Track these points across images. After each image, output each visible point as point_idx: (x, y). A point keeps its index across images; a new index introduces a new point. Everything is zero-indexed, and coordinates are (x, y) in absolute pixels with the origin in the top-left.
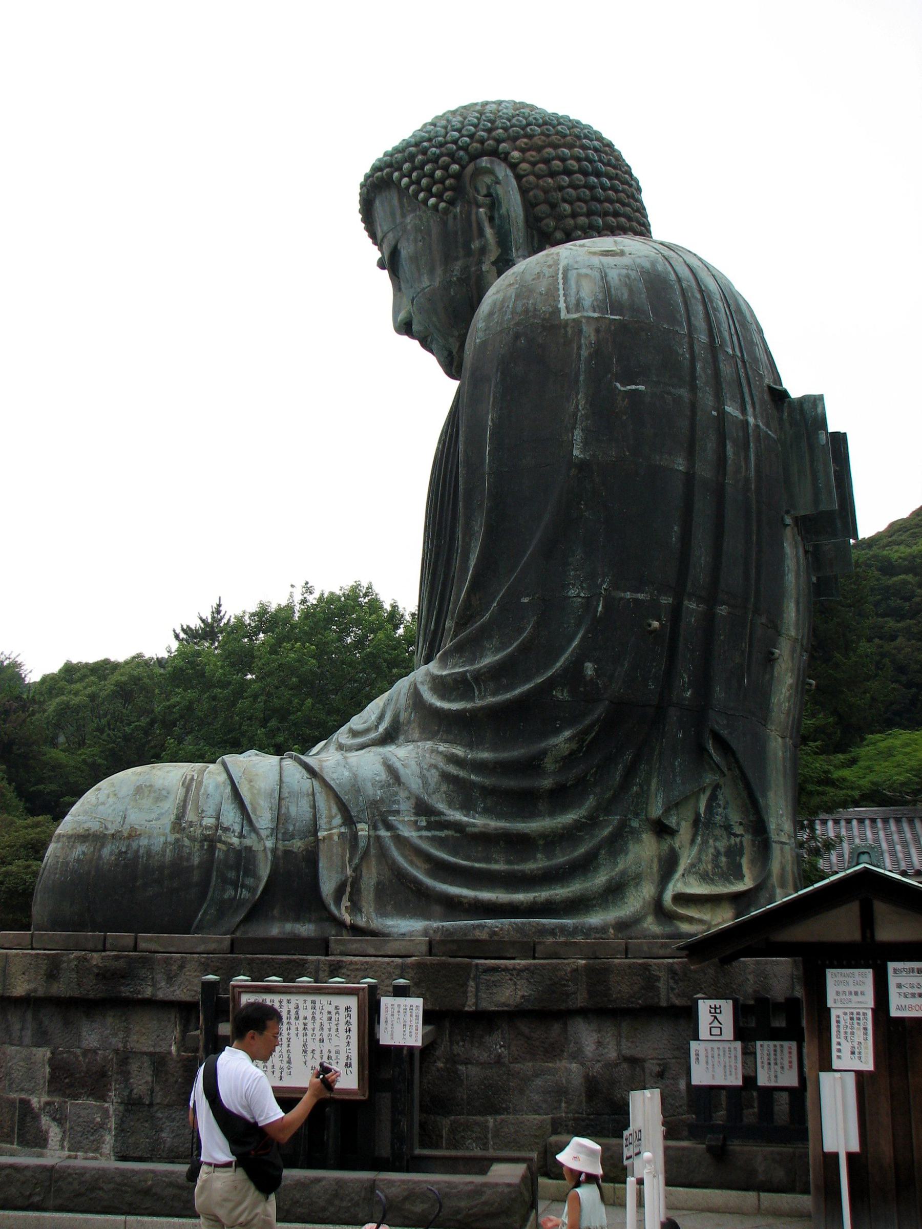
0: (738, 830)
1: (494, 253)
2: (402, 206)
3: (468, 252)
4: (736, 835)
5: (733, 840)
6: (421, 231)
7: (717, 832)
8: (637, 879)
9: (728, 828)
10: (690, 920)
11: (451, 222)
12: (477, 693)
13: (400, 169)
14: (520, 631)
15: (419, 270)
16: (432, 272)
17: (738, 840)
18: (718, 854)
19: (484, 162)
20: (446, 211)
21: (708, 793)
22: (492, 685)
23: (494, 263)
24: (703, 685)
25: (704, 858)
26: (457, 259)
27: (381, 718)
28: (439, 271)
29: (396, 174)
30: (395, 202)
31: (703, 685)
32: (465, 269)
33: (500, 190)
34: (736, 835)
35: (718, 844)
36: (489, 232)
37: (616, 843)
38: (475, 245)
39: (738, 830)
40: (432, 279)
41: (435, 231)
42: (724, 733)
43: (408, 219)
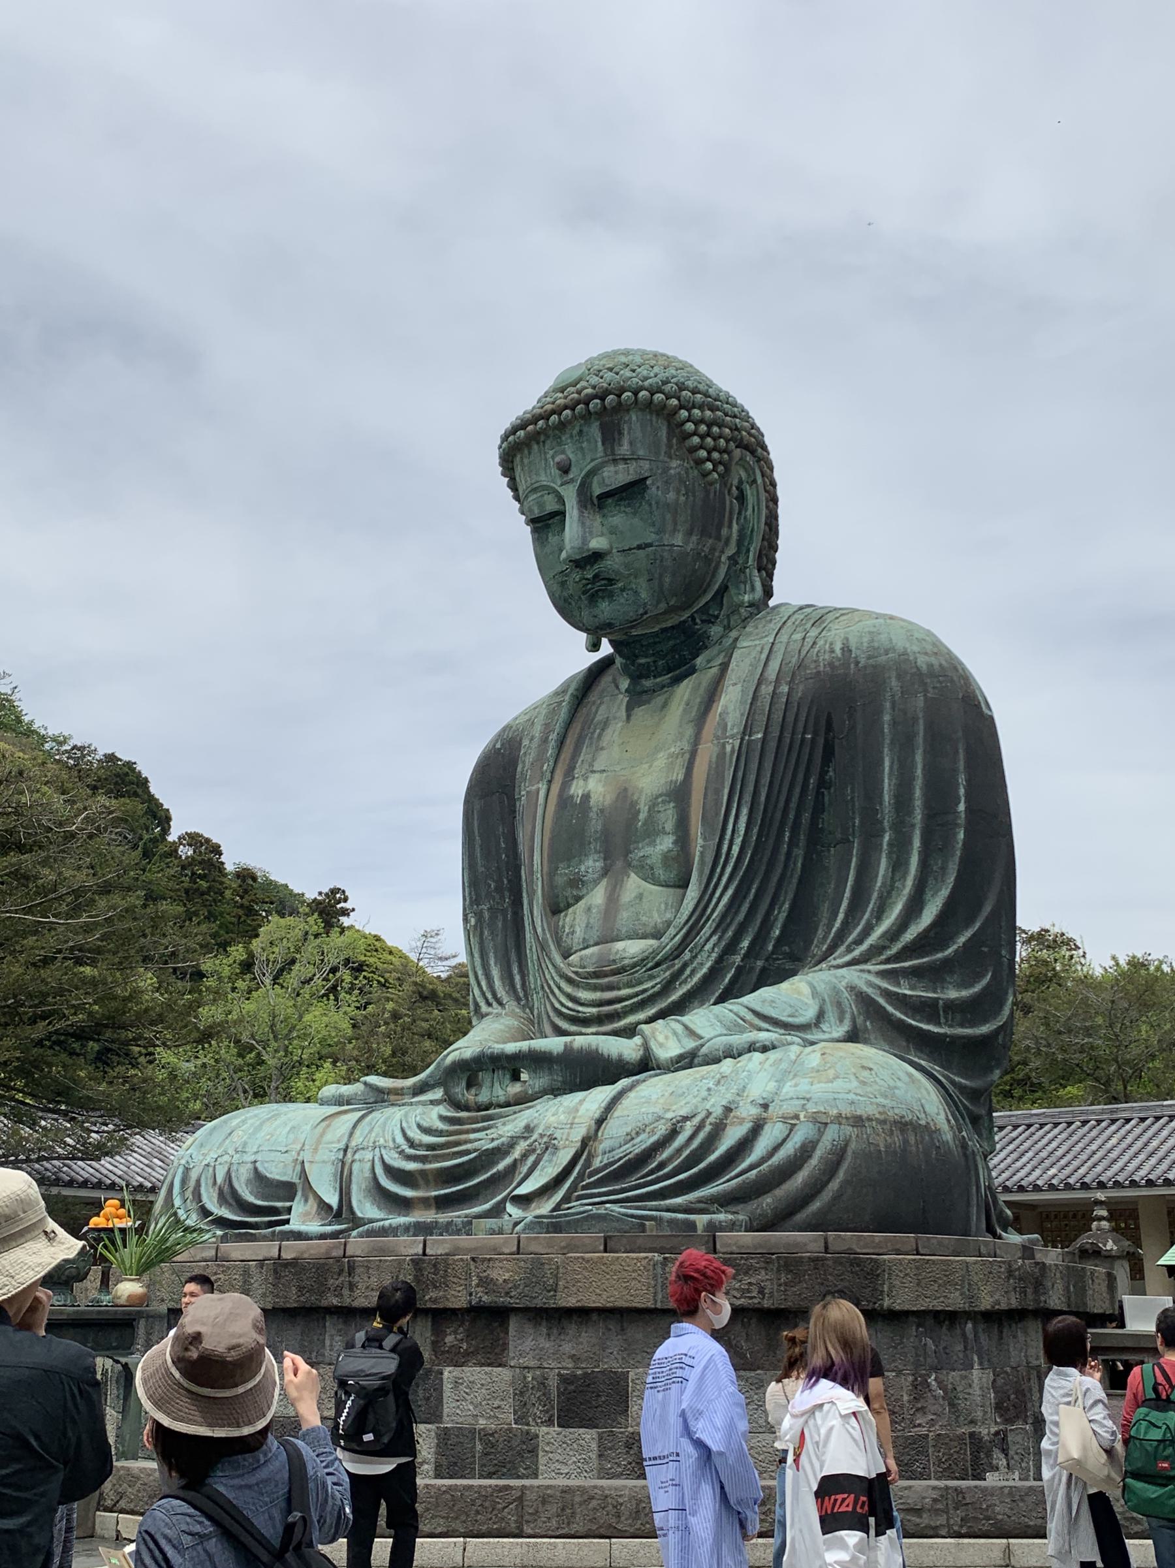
1: (731, 550)
2: (670, 446)
3: (718, 538)
6: (686, 486)
11: (712, 495)
12: (942, 1020)
13: (689, 410)
14: (979, 976)
15: (675, 524)
16: (690, 533)
19: (749, 457)
20: (711, 484)
22: (958, 1016)
23: (729, 558)
26: (710, 537)
27: (820, 1016)
28: (694, 538)
29: (684, 414)
30: (663, 433)
32: (713, 549)
33: (749, 491)
36: (735, 527)
38: (724, 531)
40: (686, 542)
41: (700, 495)
43: (674, 463)
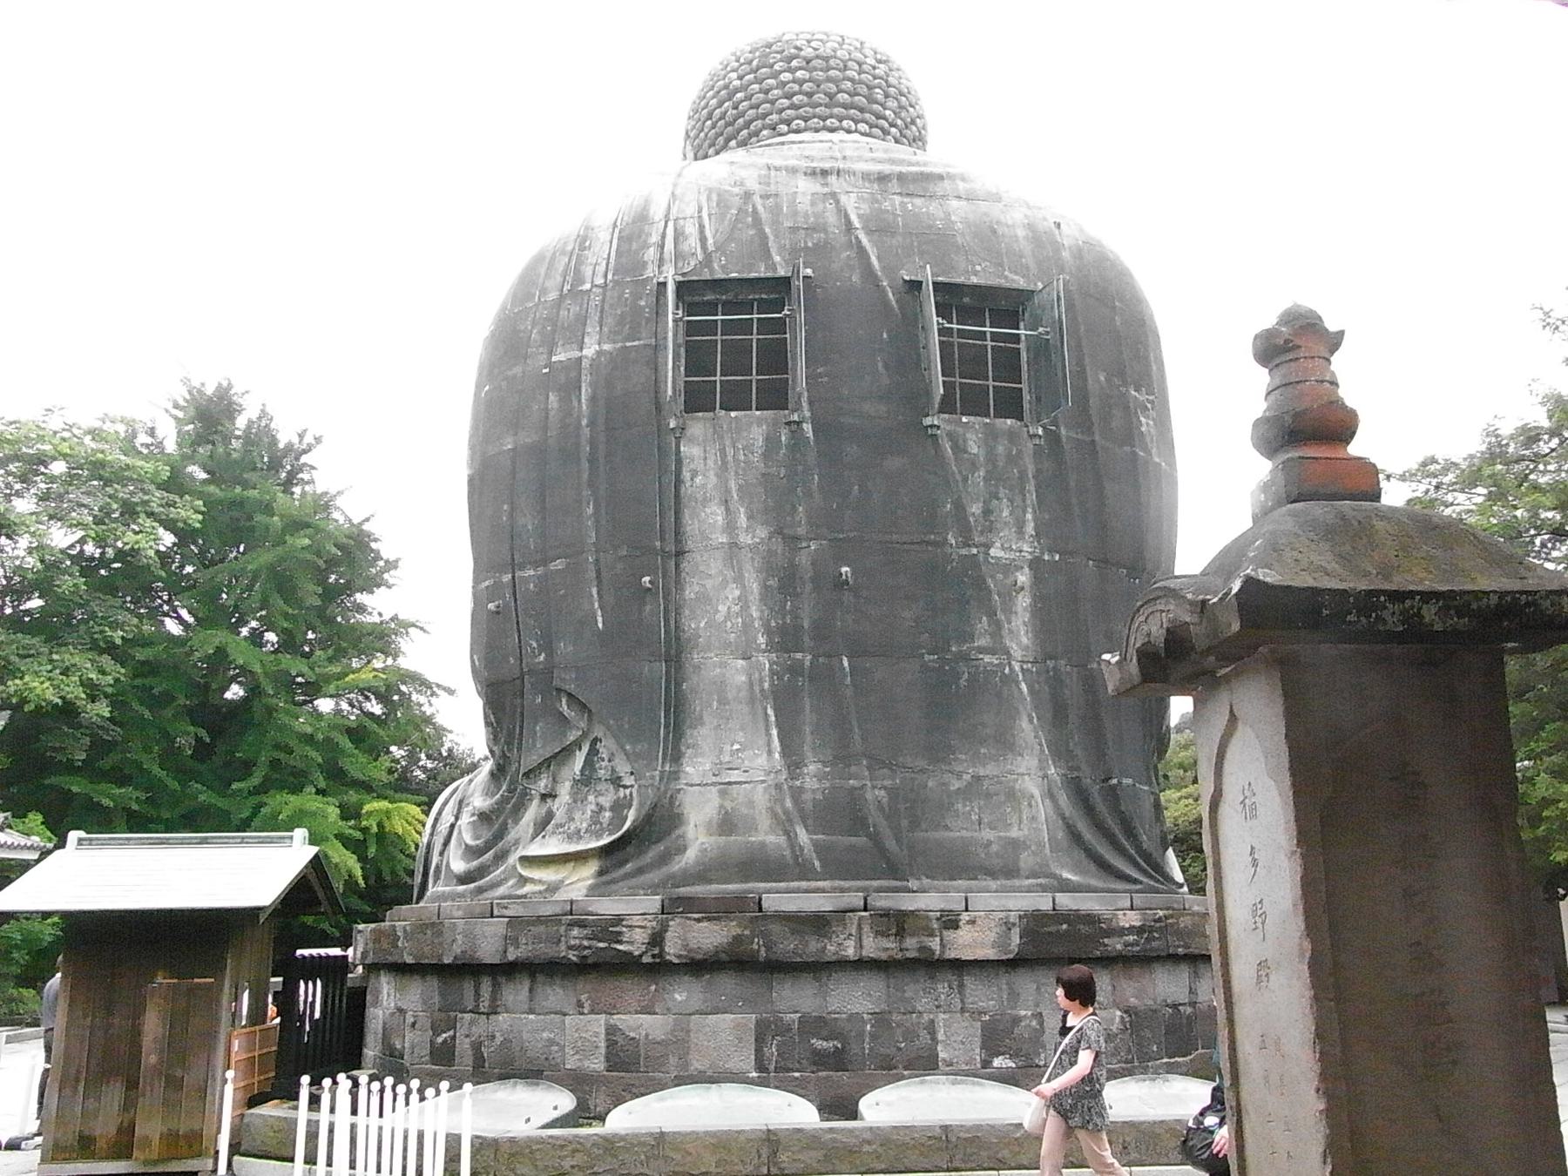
0: (628, 781)
4: (625, 787)
5: (622, 792)
7: (602, 787)
8: (517, 842)
9: (616, 781)
10: (532, 881)
17: (628, 791)
18: (601, 808)
21: (585, 749)
24: (548, 646)
25: (577, 816)
31: (548, 646)
34: (625, 787)
35: (601, 800)
37: (519, 810)
39: (628, 781)
42: (571, 688)
